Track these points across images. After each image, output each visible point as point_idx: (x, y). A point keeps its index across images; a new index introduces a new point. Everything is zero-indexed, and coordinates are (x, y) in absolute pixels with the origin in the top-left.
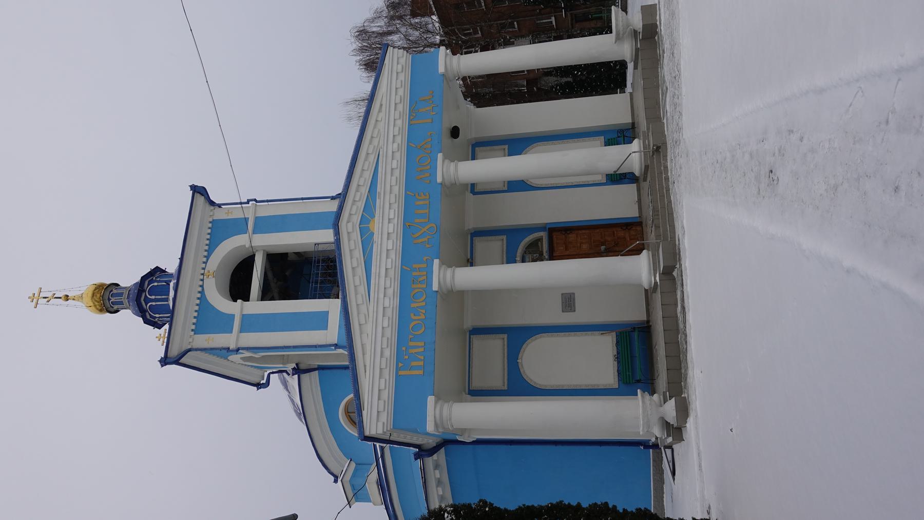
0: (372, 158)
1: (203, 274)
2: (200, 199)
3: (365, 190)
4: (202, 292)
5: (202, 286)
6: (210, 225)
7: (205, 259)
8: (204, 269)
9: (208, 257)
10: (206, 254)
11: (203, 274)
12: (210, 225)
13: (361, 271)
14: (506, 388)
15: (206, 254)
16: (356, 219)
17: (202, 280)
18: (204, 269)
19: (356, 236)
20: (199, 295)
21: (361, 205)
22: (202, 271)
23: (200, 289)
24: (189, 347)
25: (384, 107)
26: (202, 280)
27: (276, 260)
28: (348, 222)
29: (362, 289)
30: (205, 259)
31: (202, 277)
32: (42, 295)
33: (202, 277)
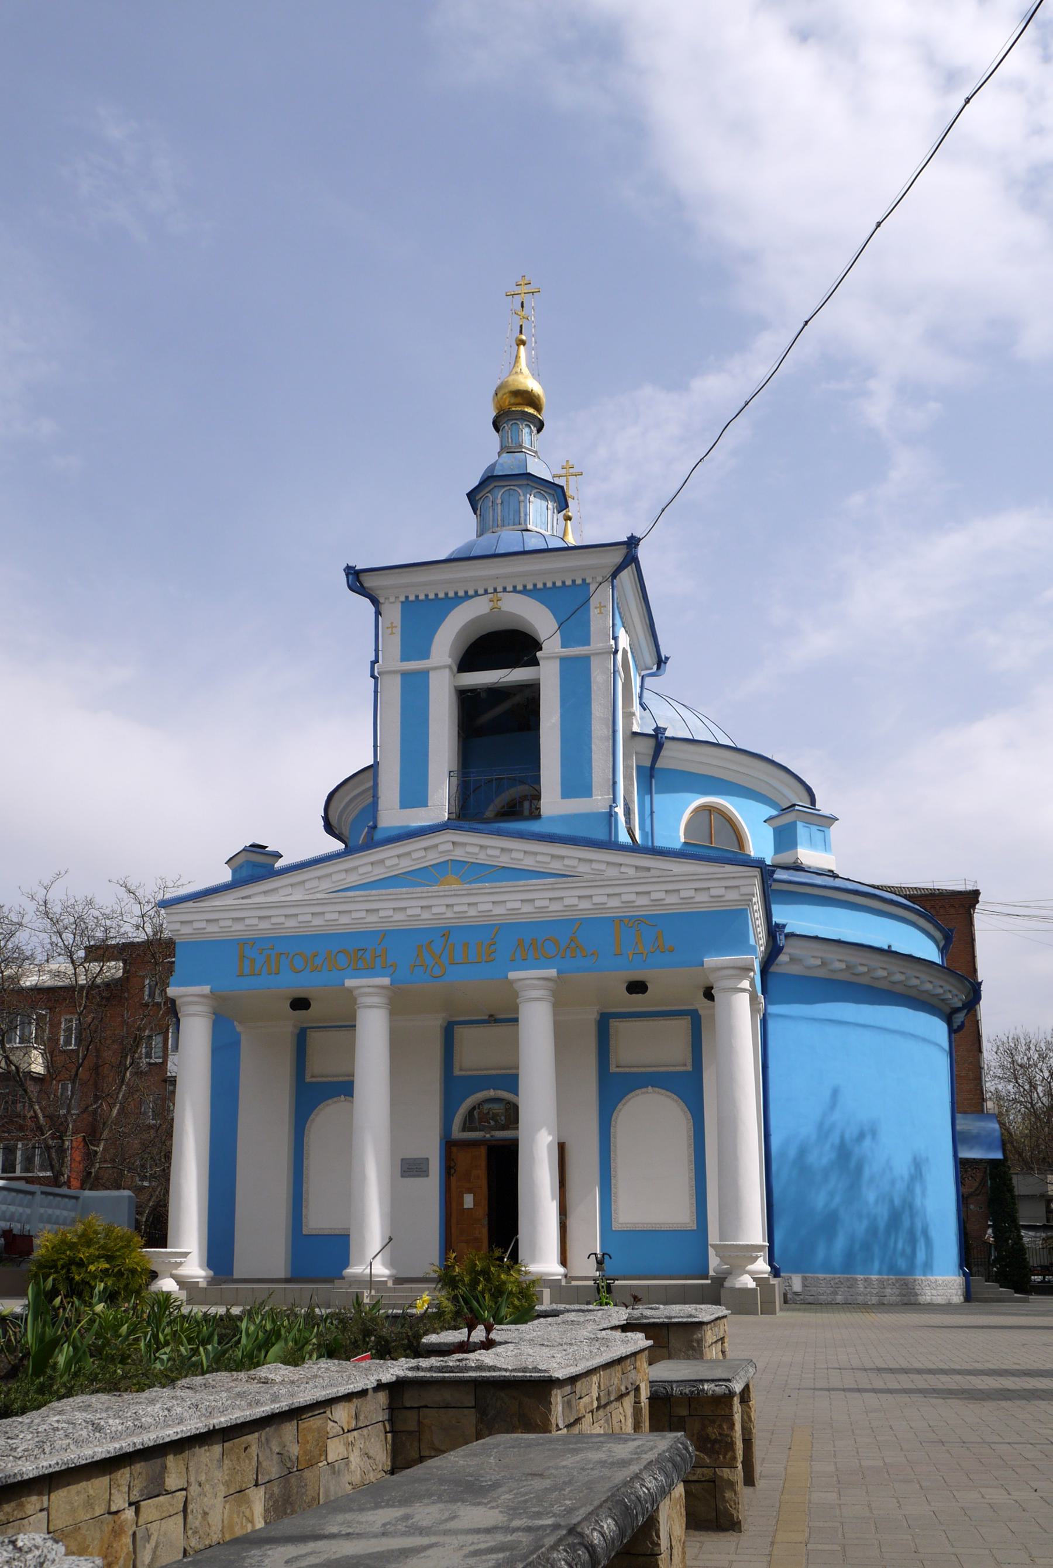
0: (556, 866)
1: (495, 590)
2: (616, 557)
3: (504, 860)
4: (467, 597)
5: (476, 594)
6: (579, 582)
7: (520, 588)
8: (505, 590)
9: (525, 591)
10: (530, 587)
11: (495, 590)
12: (579, 582)
13: (379, 873)
14: (308, 1079)
15: (530, 587)
16: (459, 854)
17: (486, 592)
18: (505, 590)
20: (461, 593)
21: (482, 858)
22: (500, 589)
23: (471, 593)
24: (381, 600)
25: (647, 874)
26: (486, 592)
27: (528, 700)
28: (453, 843)
29: (353, 879)
30: (520, 588)
31: (490, 590)
32: (527, 299)
33: (490, 590)
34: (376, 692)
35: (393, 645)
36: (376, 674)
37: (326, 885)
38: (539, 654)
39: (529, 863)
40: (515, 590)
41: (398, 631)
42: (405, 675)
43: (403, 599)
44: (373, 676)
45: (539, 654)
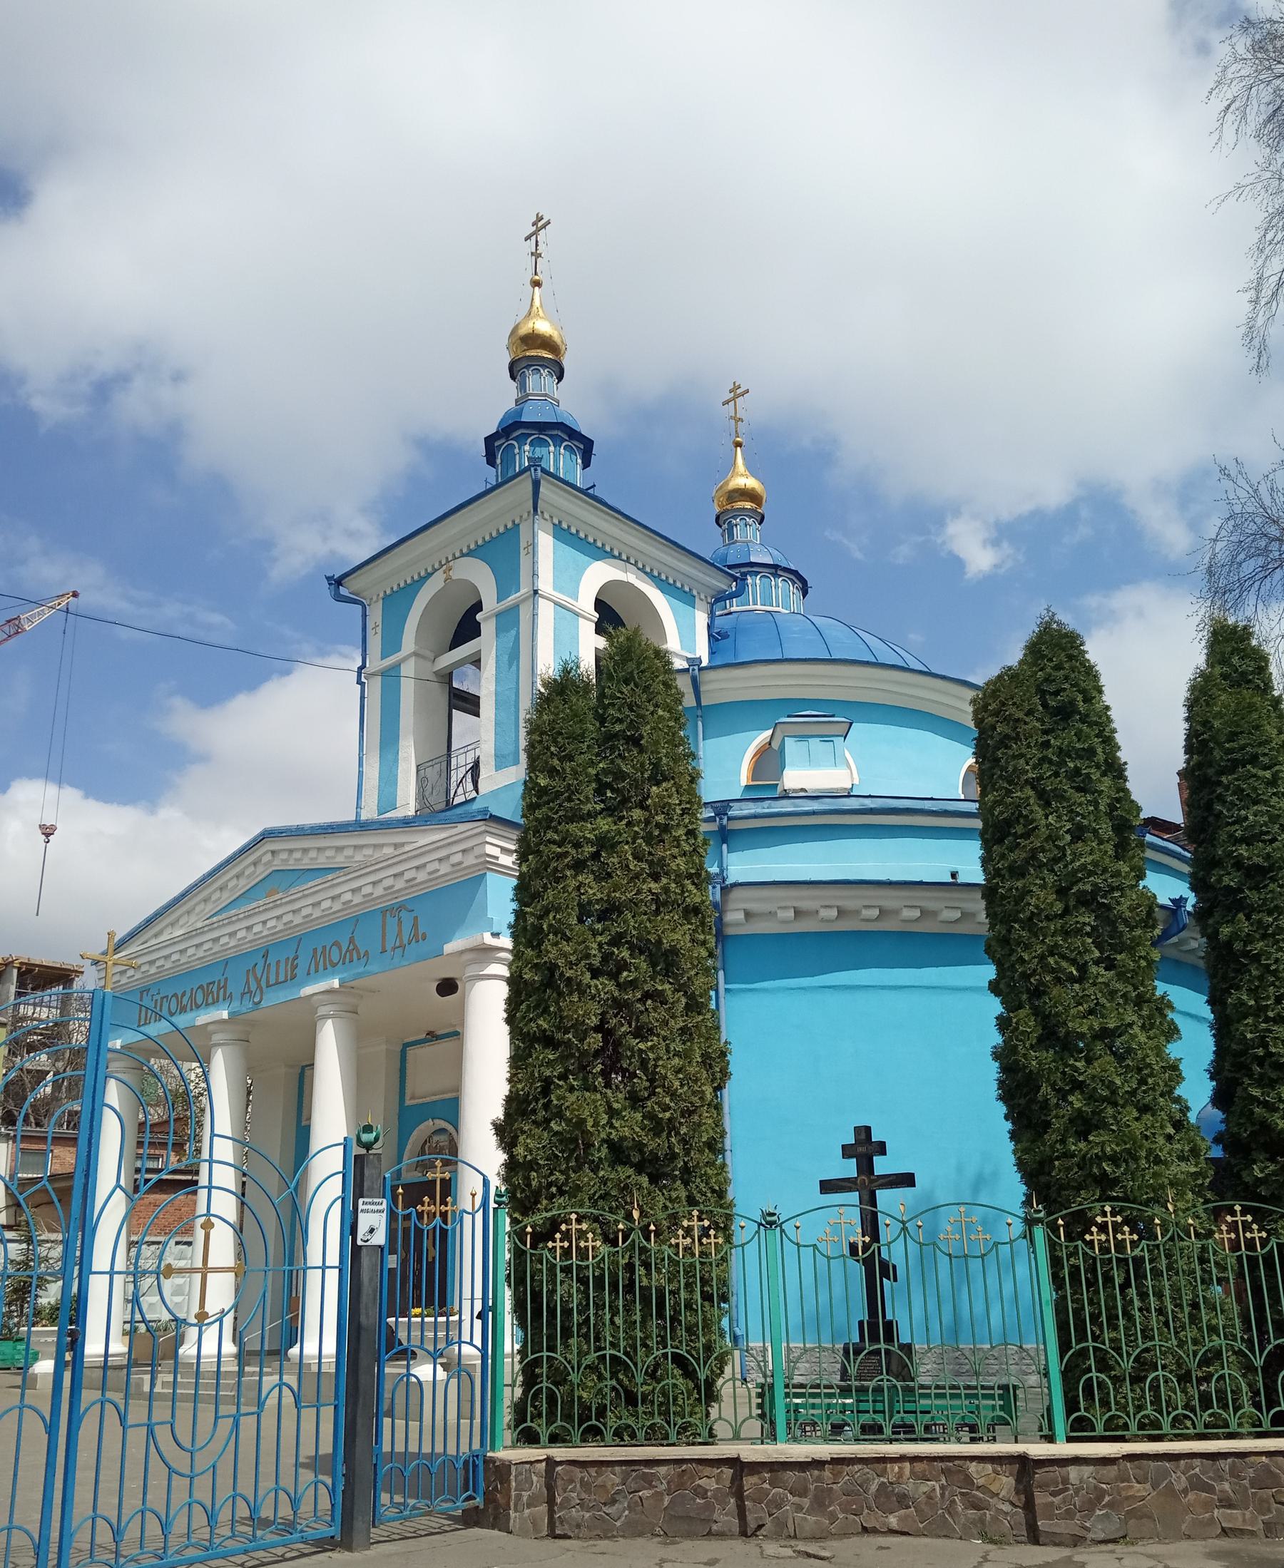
4: (429, 575)
6: (510, 525)
7: (465, 551)
9: (470, 553)
12: (510, 525)
16: (277, 864)
18: (455, 558)
19: (262, 872)
34: (362, 698)
35: (375, 642)
36: (363, 680)
37: (193, 918)
38: (479, 617)
39: (322, 861)
40: (463, 555)
41: (379, 630)
42: (384, 673)
43: (382, 595)
44: (359, 682)
45: (479, 617)
